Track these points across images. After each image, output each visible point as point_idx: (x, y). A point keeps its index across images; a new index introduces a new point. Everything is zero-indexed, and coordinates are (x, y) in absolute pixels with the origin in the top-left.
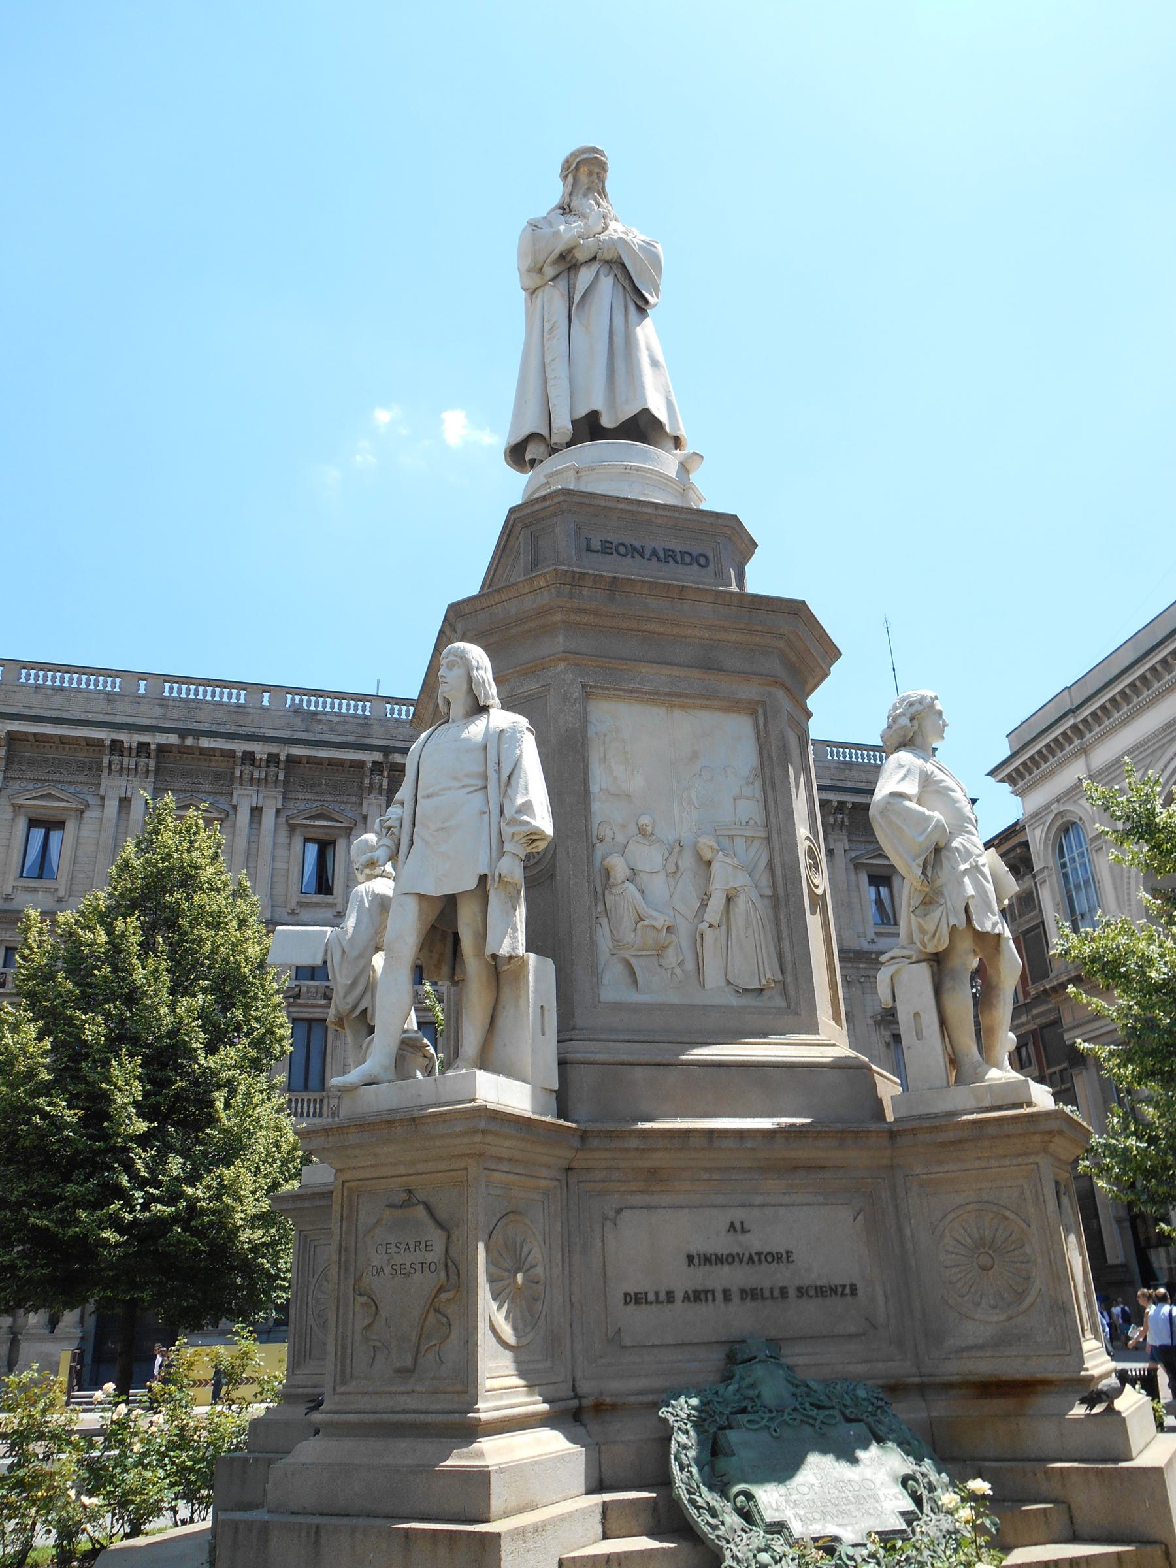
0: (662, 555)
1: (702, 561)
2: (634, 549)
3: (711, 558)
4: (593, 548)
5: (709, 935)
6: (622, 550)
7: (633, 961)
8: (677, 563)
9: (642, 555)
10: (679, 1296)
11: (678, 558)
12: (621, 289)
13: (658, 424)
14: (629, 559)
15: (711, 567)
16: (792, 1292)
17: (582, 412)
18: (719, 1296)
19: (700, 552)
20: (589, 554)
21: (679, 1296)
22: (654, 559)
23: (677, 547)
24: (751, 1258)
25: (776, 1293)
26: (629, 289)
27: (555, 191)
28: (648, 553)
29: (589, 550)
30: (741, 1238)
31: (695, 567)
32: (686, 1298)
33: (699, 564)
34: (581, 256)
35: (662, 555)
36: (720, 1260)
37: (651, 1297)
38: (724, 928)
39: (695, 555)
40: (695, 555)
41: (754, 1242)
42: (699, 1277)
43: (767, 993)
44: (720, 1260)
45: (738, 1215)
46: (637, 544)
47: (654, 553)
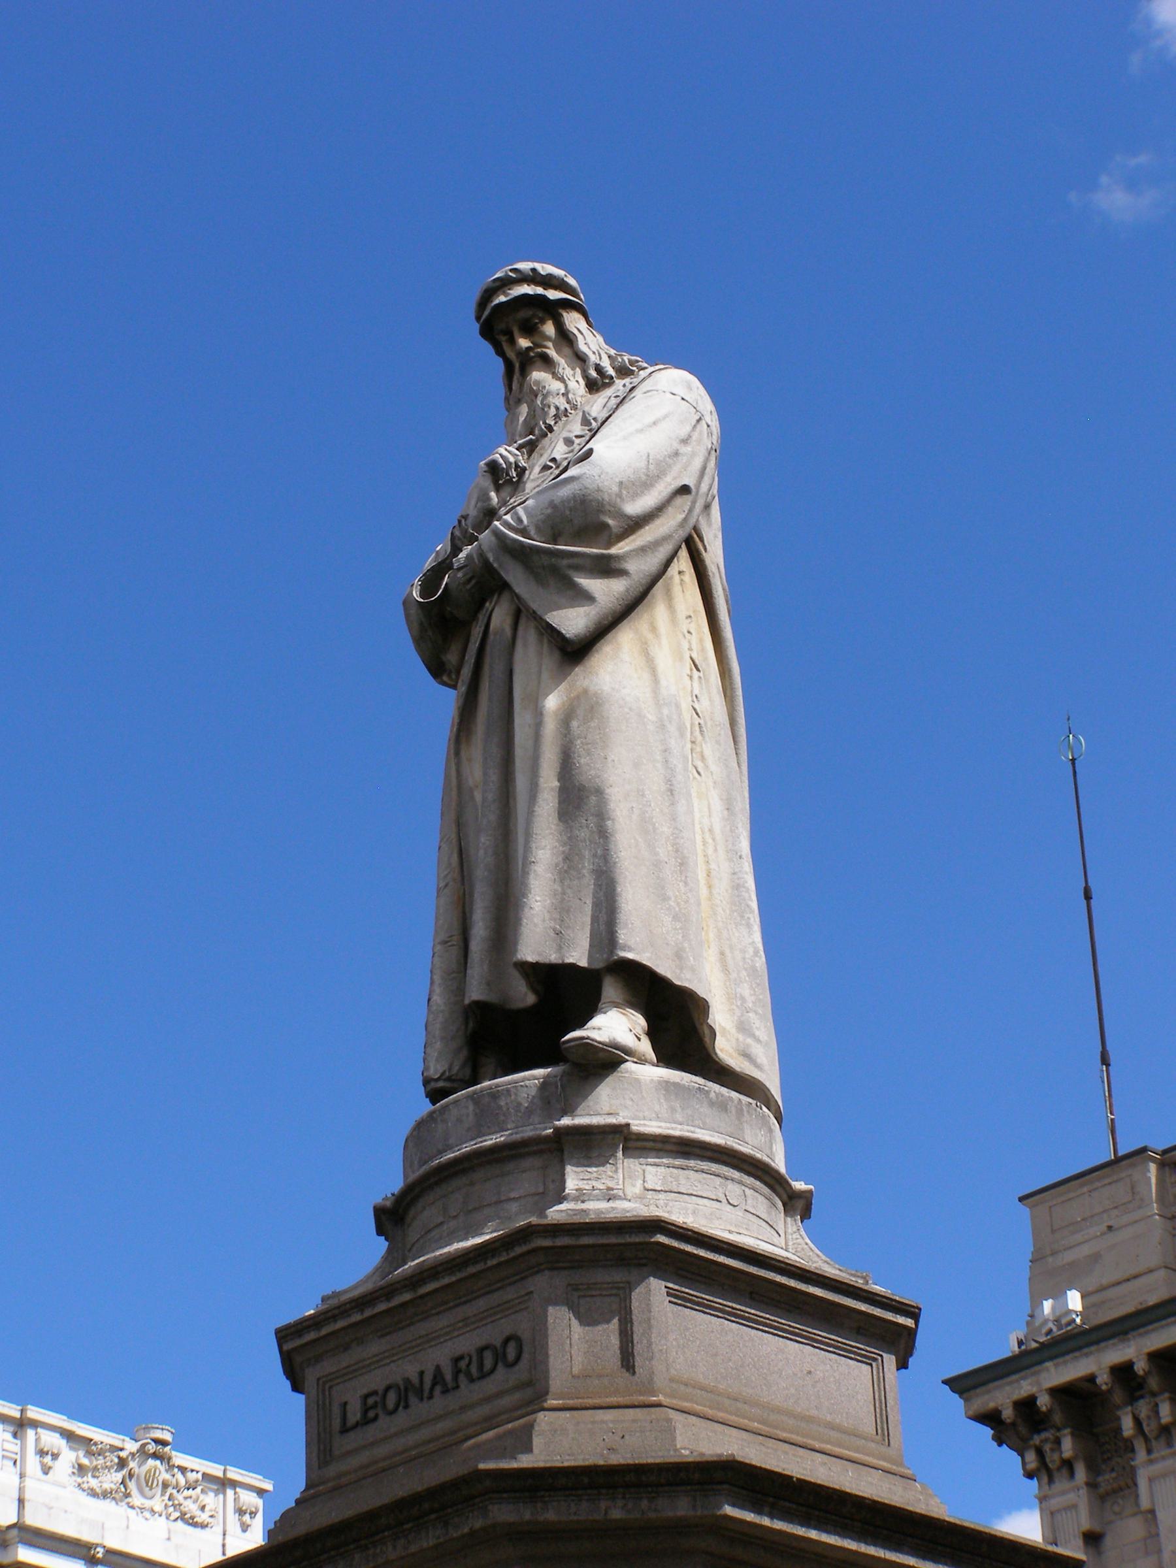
0: (448, 1377)
8: (472, 1380)
14: (402, 1419)
19: (507, 1333)
23: (466, 1343)
29: (345, 1430)
35: (448, 1377)
39: (498, 1343)
40: (498, 1343)
46: (410, 1370)
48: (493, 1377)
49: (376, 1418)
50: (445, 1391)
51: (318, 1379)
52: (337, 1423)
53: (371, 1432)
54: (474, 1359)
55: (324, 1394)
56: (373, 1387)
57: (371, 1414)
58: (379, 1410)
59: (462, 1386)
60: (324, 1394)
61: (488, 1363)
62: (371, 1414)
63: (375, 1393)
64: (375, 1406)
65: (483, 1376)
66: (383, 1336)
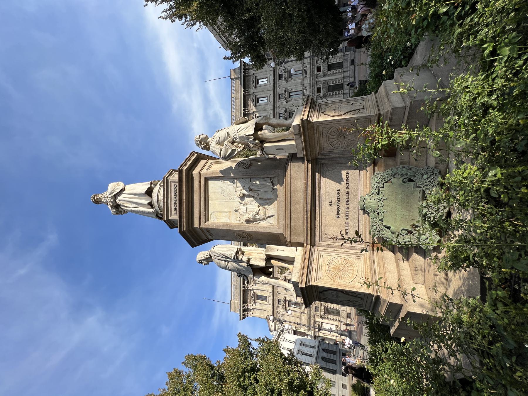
5: (260, 196)
7: (267, 216)
10: (346, 221)
13: (148, 188)
16: (347, 190)
18: (347, 210)
21: (346, 221)
24: (338, 201)
25: (347, 195)
30: (333, 202)
32: (347, 219)
34: (115, 205)
36: (338, 209)
37: (347, 228)
38: (259, 192)
41: (334, 199)
42: (342, 214)
43: (274, 182)
44: (338, 209)
45: (327, 203)
46: (173, 202)
47: (175, 198)
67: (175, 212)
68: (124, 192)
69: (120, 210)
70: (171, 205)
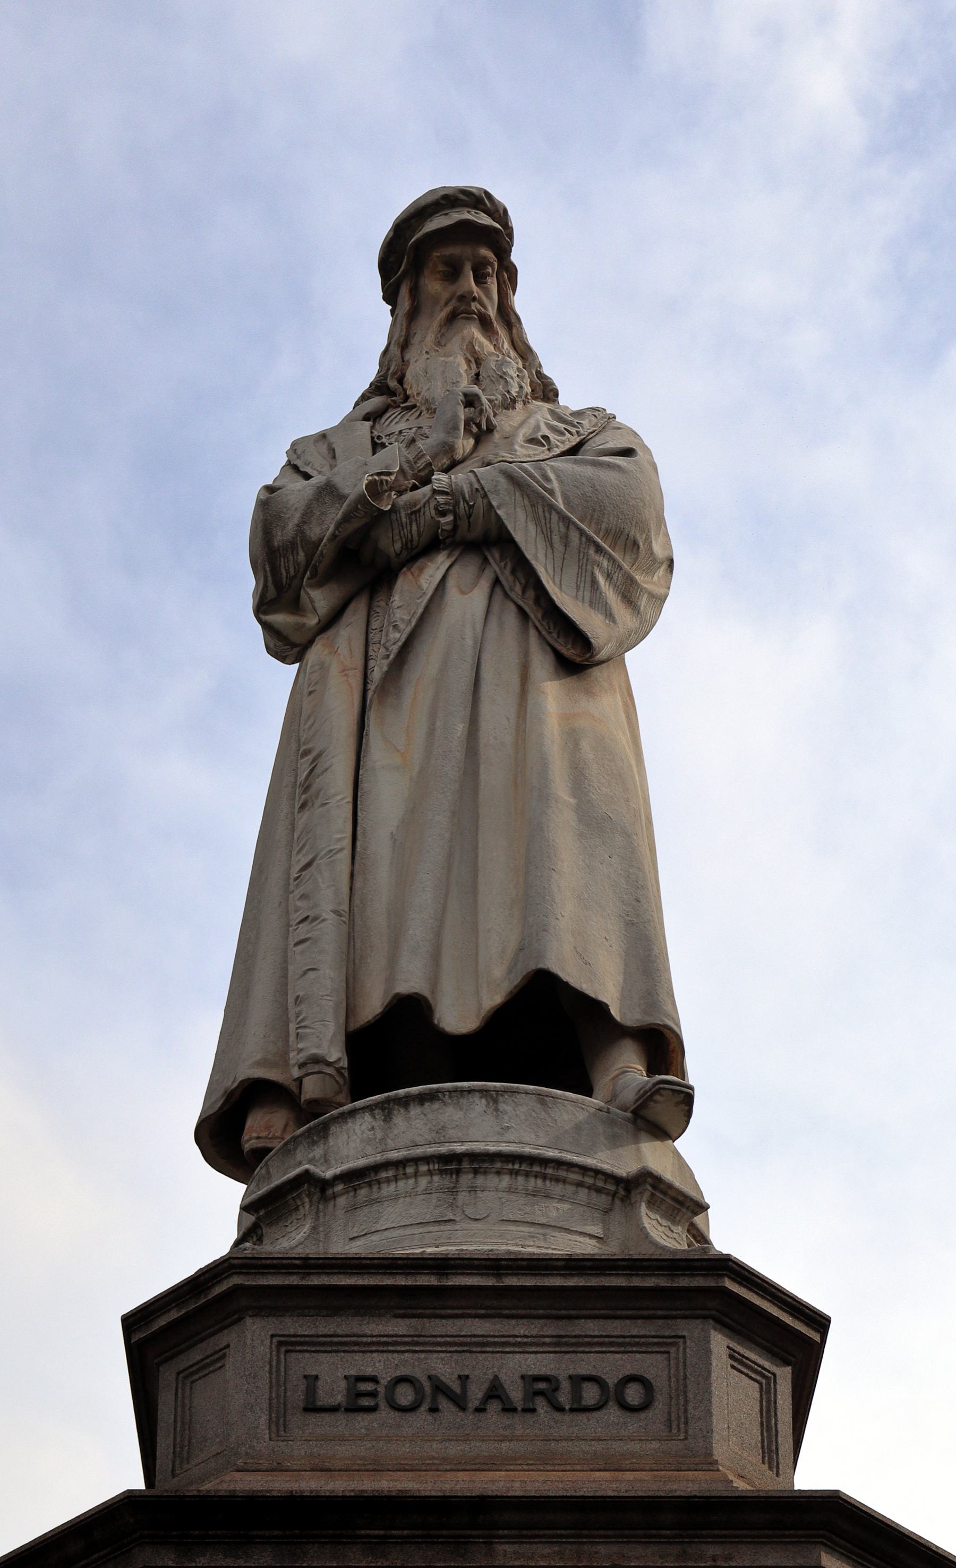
0: (516, 1394)
1: (633, 1394)
2: (439, 1388)
3: (656, 1384)
4: (324, 1399)
6: (405, 1395)
8: (560, 1409)
9: (459, 1402)
11: (564, 1398)
12: (511, 619)
15: (659, 1406)
17: (373, 1004)
19: (629, 1370)
20: (313, 1418)
22: (494, 1407)
26: (535, 615)
27: (364, 322)
28: (476, 1393)
29: (311, 1408)
31: (612, 1413)
33: (626, 1407)
34: (391, 543)
35: (516, 1394)
39: (611, 1381)
40: (611, 1381)
46: (445, 1367)
47: (495, 1392)
48: (596, 1414)
49: (373, 1409)
50: (509, 1409)
51: (272, 1336)
52: (297, 1396)
53: (362, 1422)
54: (565, 1385)
55: (278, 1356)
56: (369, 1371)
57: (366, 1402)
58: (383, 1404)
59: (541, 1411)
60: (278, 1356)
61: (591, 1394)
62: (366, 1402)
63: (374, 1379)
64: (373, 1394)
65: (579, 1409)
66: (403, 1316)
67: (333, 1389)
68: (541, 664)
69: (320, 600)
70: (415, 1344)
